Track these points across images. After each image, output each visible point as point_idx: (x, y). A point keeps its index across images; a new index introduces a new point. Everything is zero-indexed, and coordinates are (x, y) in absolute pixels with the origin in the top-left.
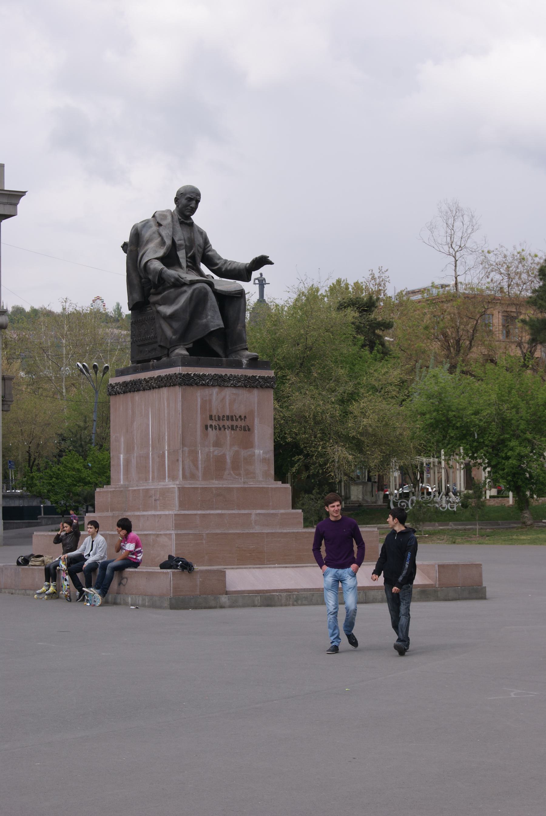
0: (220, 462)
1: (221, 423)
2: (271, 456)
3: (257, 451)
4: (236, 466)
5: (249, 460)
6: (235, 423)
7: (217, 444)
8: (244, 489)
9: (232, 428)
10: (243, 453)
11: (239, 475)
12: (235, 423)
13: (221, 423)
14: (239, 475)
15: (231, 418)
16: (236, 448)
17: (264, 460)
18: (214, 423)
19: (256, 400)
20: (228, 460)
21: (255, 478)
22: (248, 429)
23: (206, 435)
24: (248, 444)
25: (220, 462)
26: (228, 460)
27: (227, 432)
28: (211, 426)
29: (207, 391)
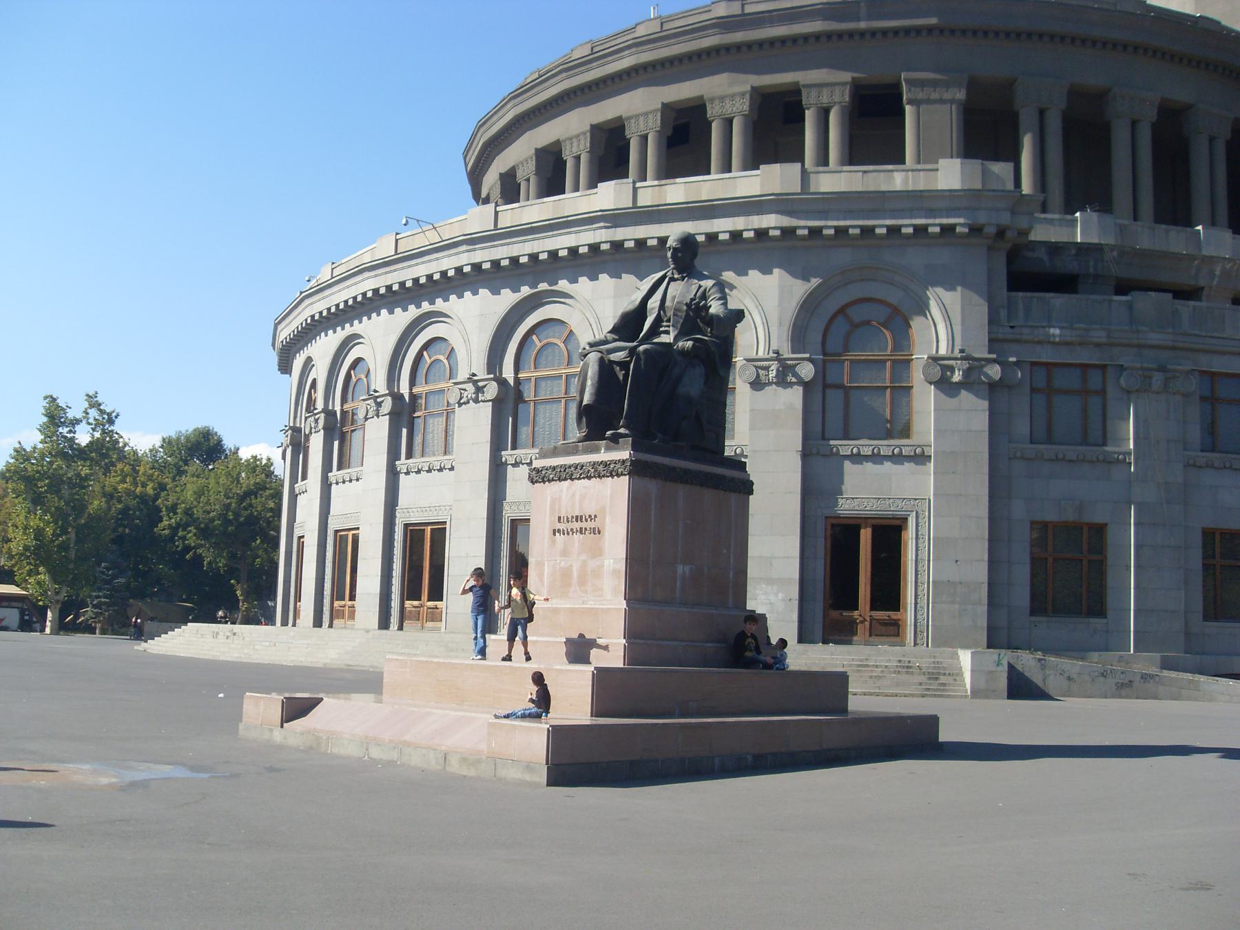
0: (566, 575)
1: (570, 526)
2: (622, 566)
3: (606, 562)
4: (582, 582)
5: (597, 574)
6: (584, 525)
7: (565, 553)
8: (572, 610)
9: (581, 531)
10: (592, 564)
11: (586, 592)
12: (584, 525)
13: (570, 526)
14: (586, 592)
15: (579, 518)
16: (583, 557)
17: (615, 571)
18: (562, 526)
19: (609, 492)
20: (575, 574)
21: (602, 596)
22: (597, 531)
23: (554, 542)
24: (597, 552)
25: (566, 575)
26: (575, 574)
27: (577, 536)
28: (559, 531)
29: (556, 486)
